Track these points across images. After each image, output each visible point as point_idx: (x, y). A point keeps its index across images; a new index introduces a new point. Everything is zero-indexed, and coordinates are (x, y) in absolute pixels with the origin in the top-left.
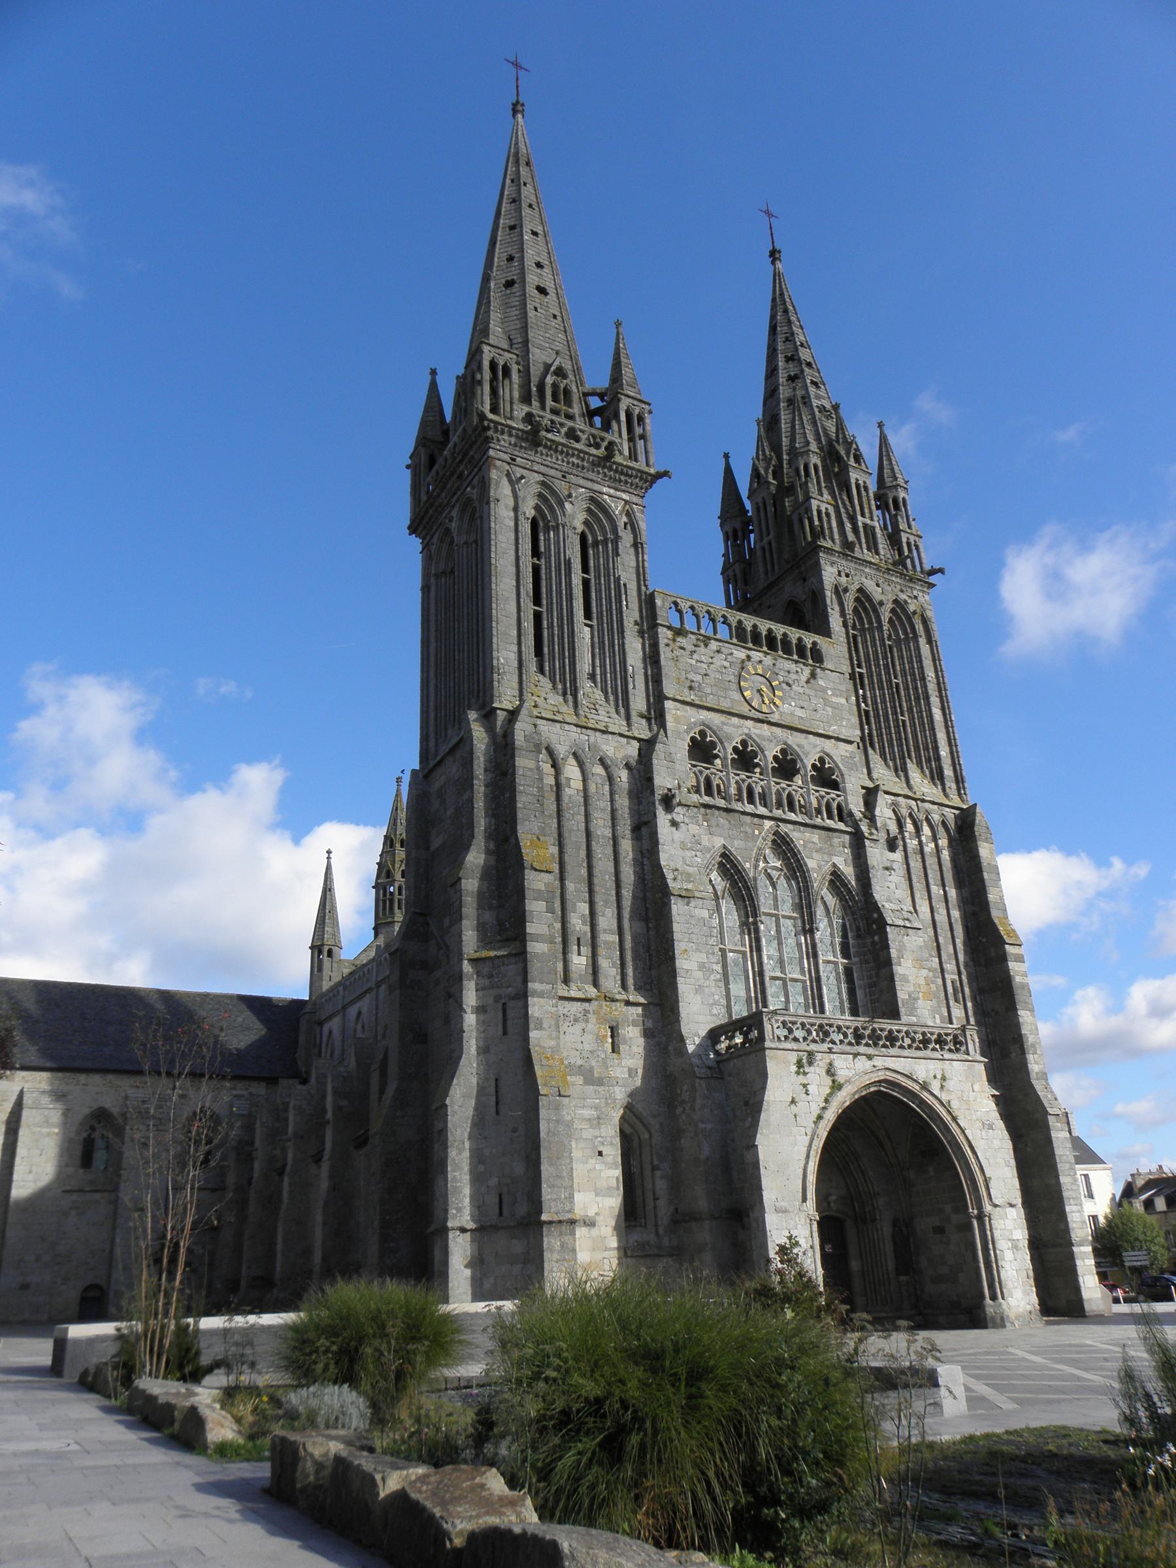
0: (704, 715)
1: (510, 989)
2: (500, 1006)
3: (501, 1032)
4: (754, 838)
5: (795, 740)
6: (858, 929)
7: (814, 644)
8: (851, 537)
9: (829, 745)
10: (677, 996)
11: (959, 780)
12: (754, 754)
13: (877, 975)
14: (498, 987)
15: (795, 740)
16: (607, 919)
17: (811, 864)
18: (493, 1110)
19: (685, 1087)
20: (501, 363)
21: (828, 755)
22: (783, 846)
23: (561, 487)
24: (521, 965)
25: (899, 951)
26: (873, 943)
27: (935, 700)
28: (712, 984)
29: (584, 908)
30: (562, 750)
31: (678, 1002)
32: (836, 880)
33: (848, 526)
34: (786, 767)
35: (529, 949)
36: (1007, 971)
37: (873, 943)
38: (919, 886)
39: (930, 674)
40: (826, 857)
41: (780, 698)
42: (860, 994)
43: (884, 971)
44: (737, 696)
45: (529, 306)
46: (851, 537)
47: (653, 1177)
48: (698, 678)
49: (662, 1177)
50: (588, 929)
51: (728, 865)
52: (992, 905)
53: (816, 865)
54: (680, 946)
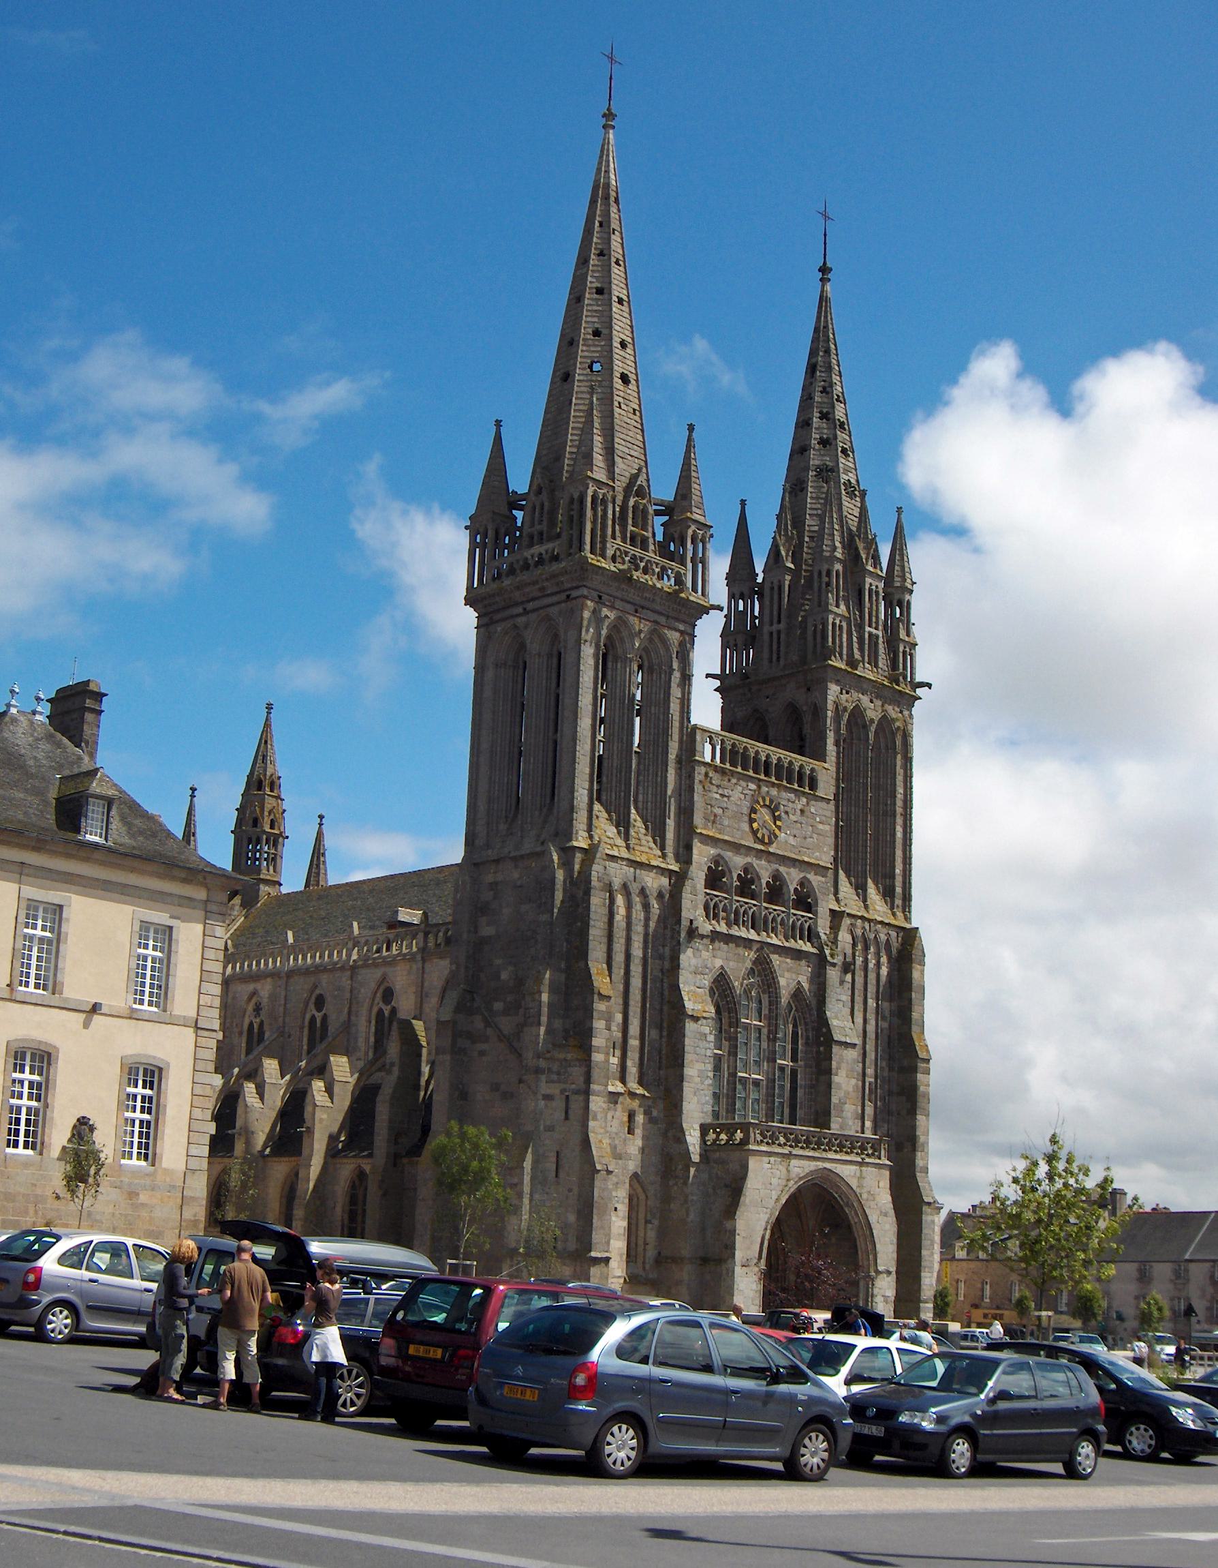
1: (573, 1086)
2: (564, 1097)
3: (563, 1117)
4: (743, 959)
6: (807, 1038)
7: (813, 770)
8: (857, 655)
10: (682, 1096)
13: (817, 1080)
14: (564, 1083)
17: (782, 982)
18: (554, 1174)
19: (680, 1167)
21: (810, 882)
24: (583, 1069)
25: (838, 1063)
26: (818, 1052)
27: (899, 820)
28: (706, 1087)
31: (682, 1101)
34: (776, 892)
35: (593, 1058)
36: (915, 1080)
37: (818, 1052)
38: (859, 999)
39: (900, 790)
40: (794, 976)
41: (779, 828)
42: (800, 1093)
43: (823, 1078)
44: (746, 827)
47: (645, 1229)
48: (720, 811)
49: (651, 1229)
50: (620, 1035)
52: (913, 1022)
54: (688, 1057)
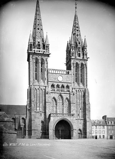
0: (53, 83)
5: (63, 84)
9: (68, 84)
11: (87, 85)
12: (59, 86)
15: (63, 84)
16: (41, 105)
20: (31, 44)
22: (61, 95)
23: (38, 58)
29: (39, 103)
30: (37, 89)
32: (67, 98)
33: (76, 54)
45: (36, 32)
46: (77, 56)
51: (54, 98)
53: (65, 98)
